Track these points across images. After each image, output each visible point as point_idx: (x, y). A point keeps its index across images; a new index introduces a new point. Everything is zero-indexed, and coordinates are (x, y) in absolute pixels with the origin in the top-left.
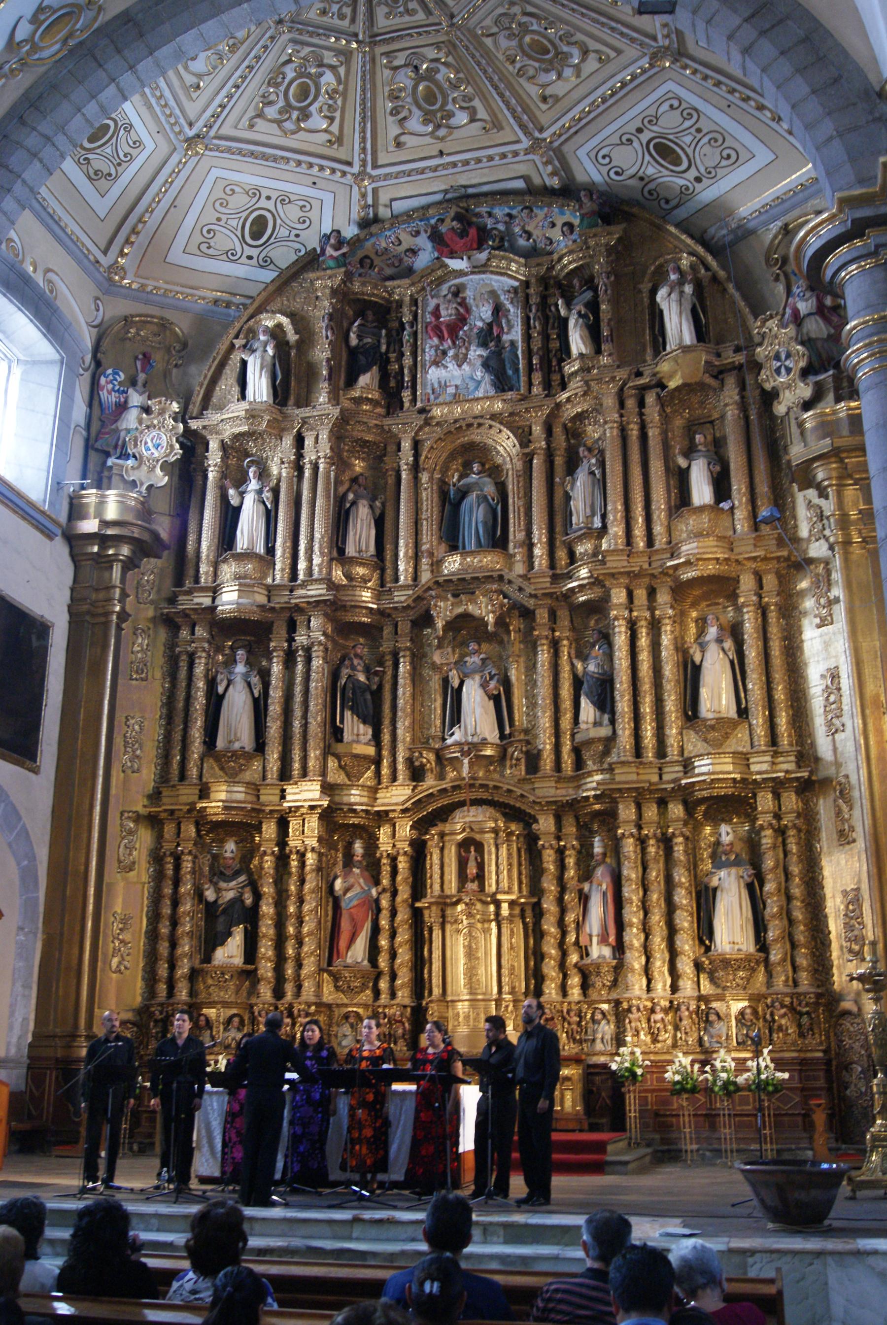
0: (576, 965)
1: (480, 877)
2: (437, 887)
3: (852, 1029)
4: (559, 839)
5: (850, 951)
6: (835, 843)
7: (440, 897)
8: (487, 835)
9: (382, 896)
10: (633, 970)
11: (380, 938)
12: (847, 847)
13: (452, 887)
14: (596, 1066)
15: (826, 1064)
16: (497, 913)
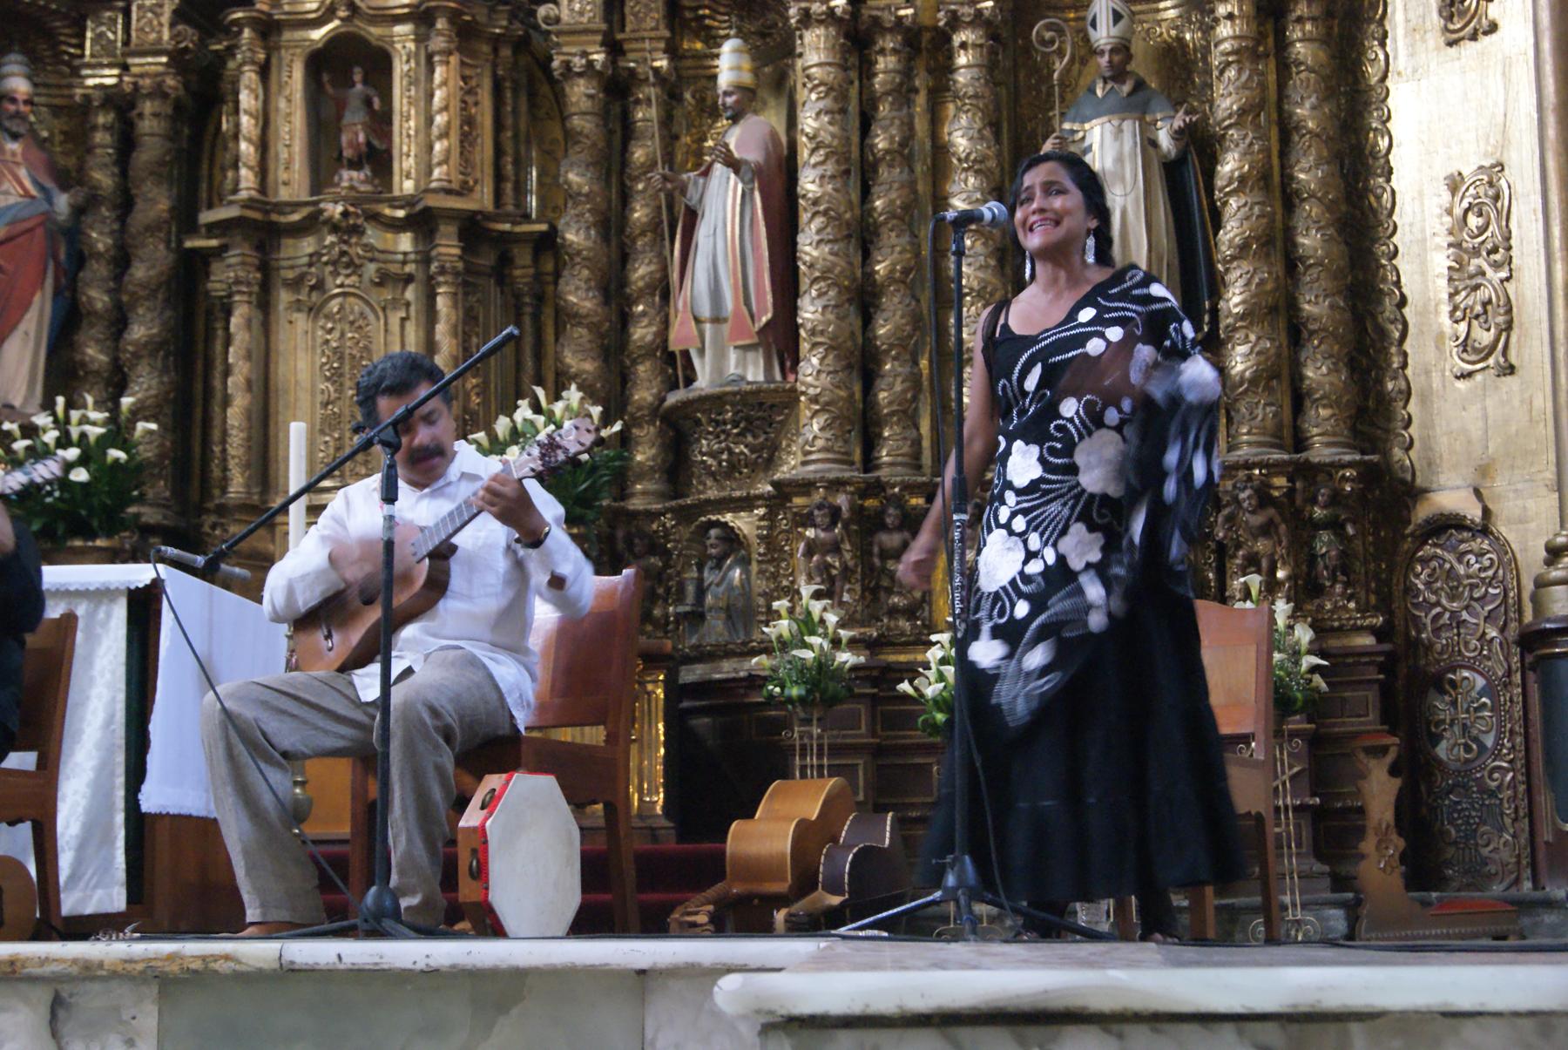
0: (657, 411)
1: (378, 160)
2: (247, 177)
3: (1461, 570)
4: (614, 49)
5: (1465, 345)
6: (1435, 39)
7: (249, 204)
8: (400, 29)
9: (88, 219)
10: (823, 404)
11: (81, 337)
12: (1468, 48)
13: (292, 181)
14: (703, 688)
15: (1382, 668)
16: (425, 260)
